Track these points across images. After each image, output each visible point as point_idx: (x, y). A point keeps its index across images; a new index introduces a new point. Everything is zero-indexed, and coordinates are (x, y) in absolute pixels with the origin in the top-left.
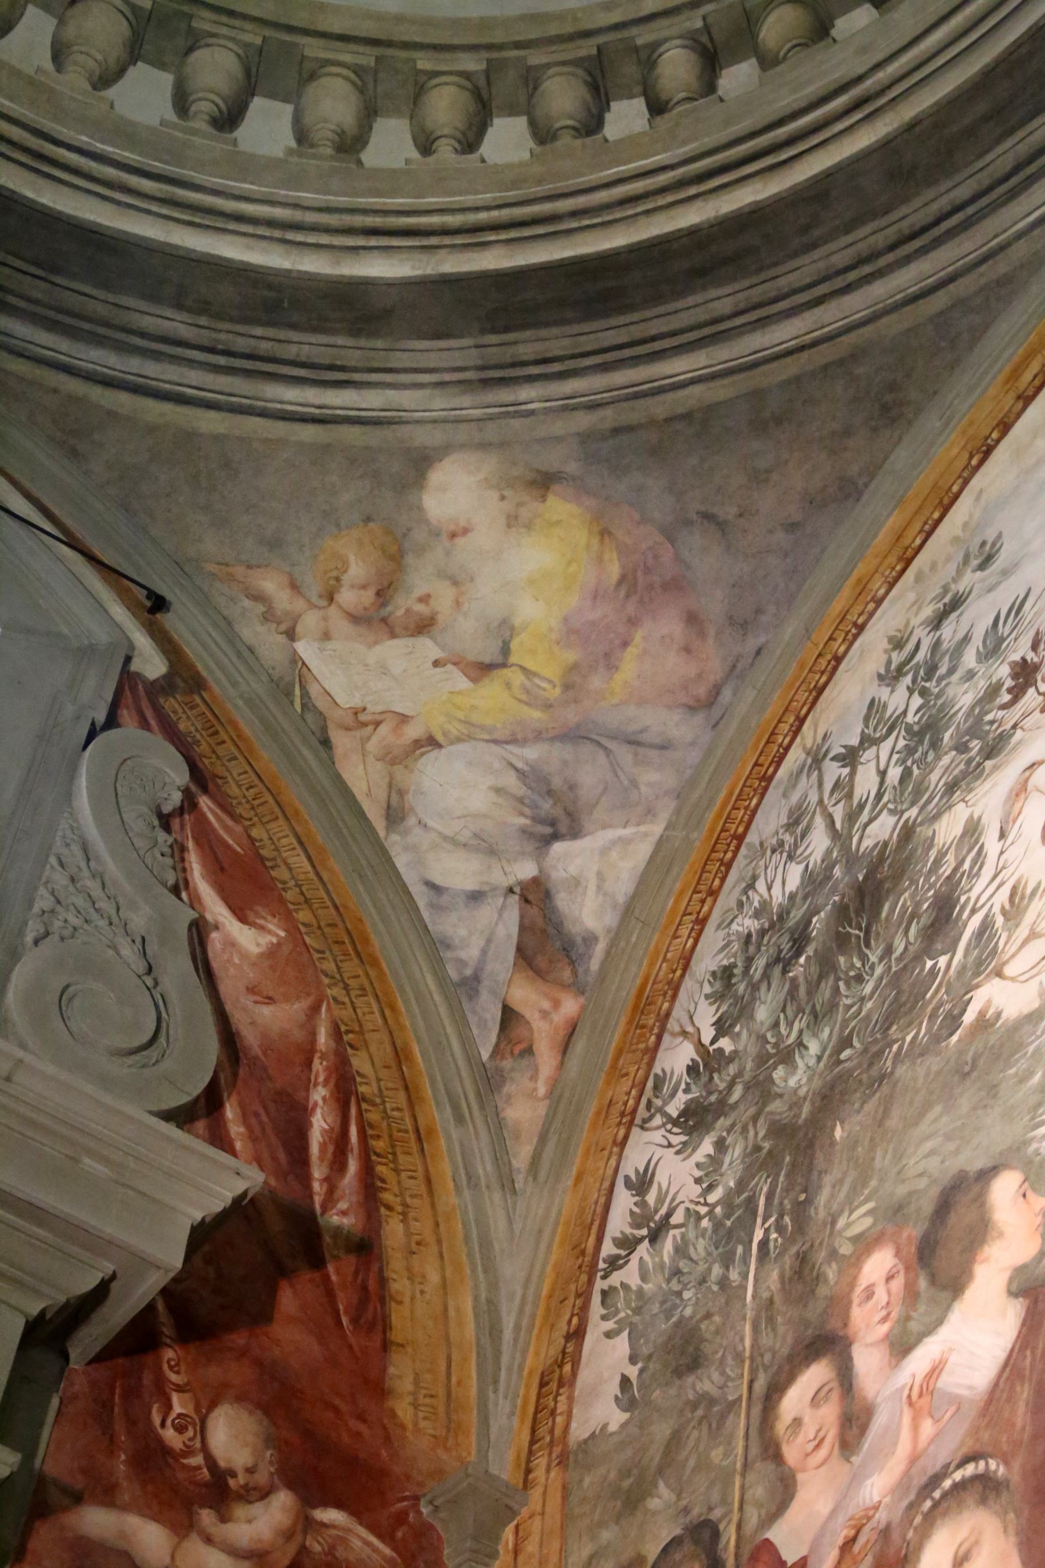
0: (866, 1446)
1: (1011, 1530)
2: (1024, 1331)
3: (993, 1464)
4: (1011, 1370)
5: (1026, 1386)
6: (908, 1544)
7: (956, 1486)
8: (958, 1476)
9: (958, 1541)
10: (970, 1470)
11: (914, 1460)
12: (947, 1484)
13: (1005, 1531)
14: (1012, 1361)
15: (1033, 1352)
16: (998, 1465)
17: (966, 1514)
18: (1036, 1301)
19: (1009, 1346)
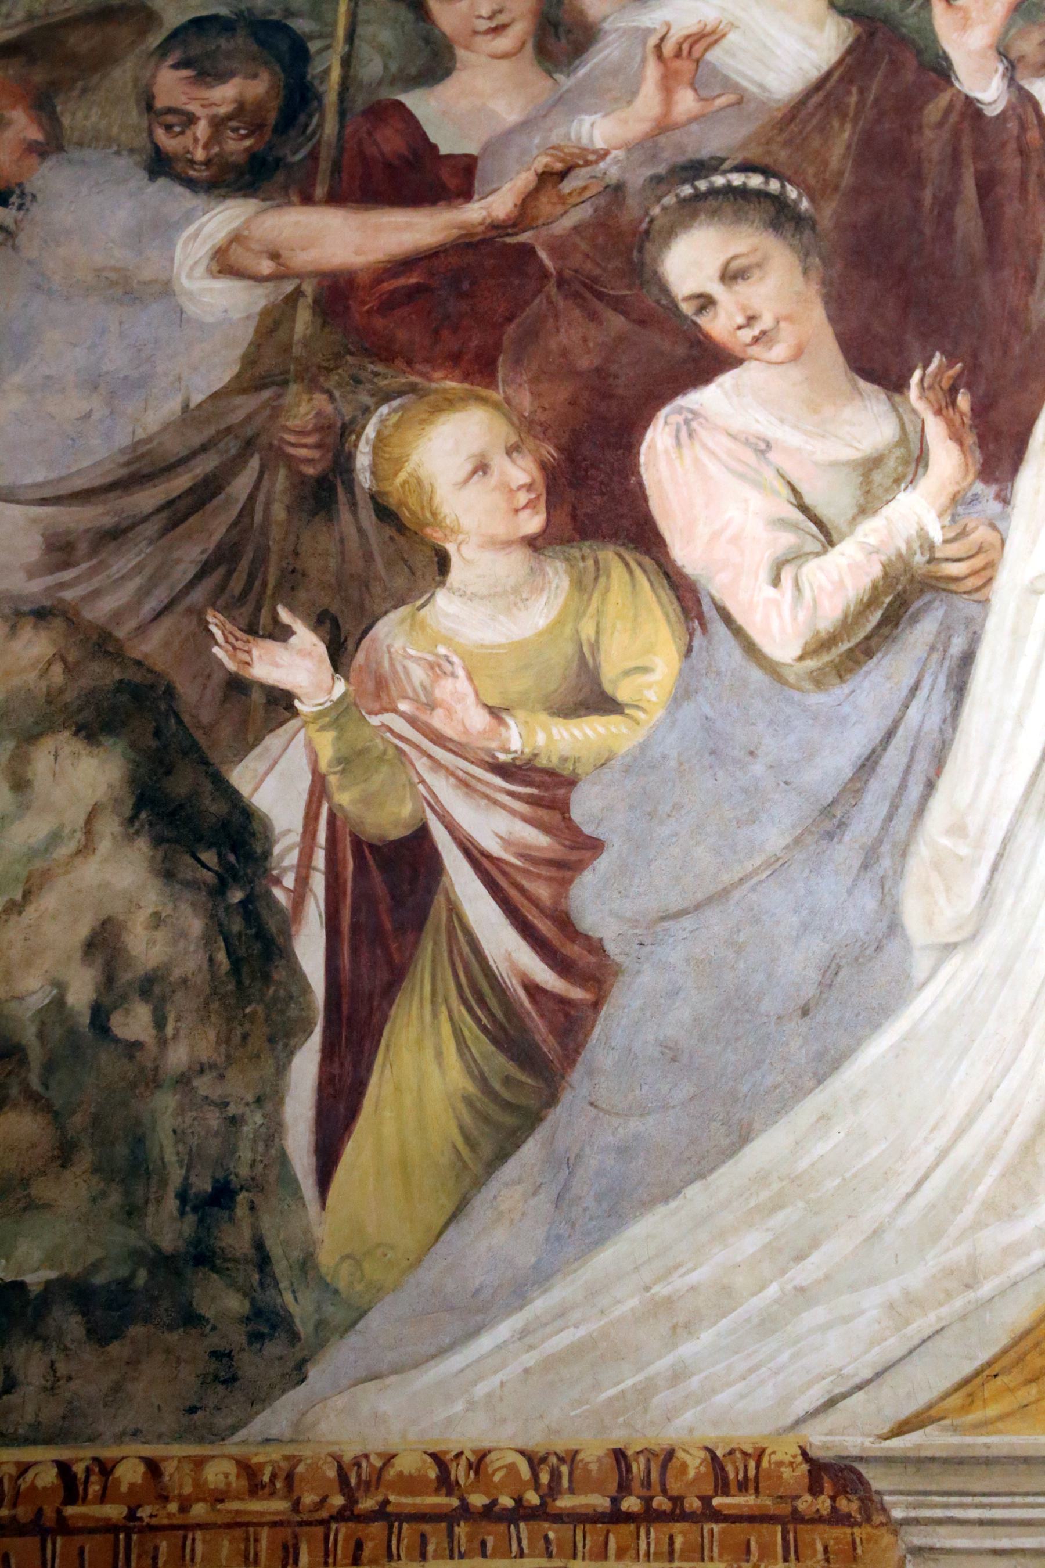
0: (582, 72)
1: (814, 275)
2: (849, 60)
3: (792, 193)
4: (827, 97)
5: (848, 126)
6: (651, 221)
7: (729, 190)
8: (737, 179)
9: (730, 254)
10: (755, 181)
11: (663, 127)
12: (719, 181)
13: (805, 272)
14: (828, 86)
15: (862, 91)
16: (800, 195)
17: (745, 229)
18: (871, 35)
19: (825, 68)
